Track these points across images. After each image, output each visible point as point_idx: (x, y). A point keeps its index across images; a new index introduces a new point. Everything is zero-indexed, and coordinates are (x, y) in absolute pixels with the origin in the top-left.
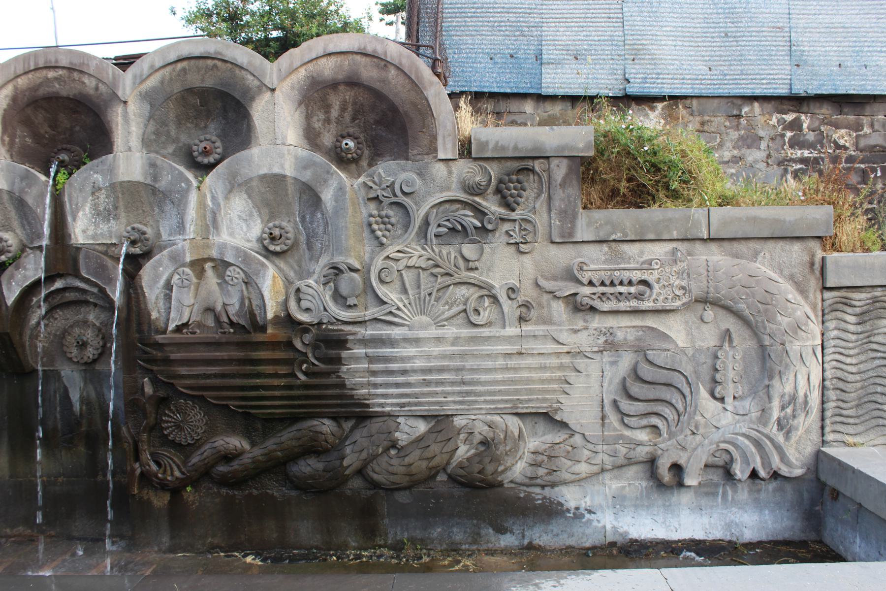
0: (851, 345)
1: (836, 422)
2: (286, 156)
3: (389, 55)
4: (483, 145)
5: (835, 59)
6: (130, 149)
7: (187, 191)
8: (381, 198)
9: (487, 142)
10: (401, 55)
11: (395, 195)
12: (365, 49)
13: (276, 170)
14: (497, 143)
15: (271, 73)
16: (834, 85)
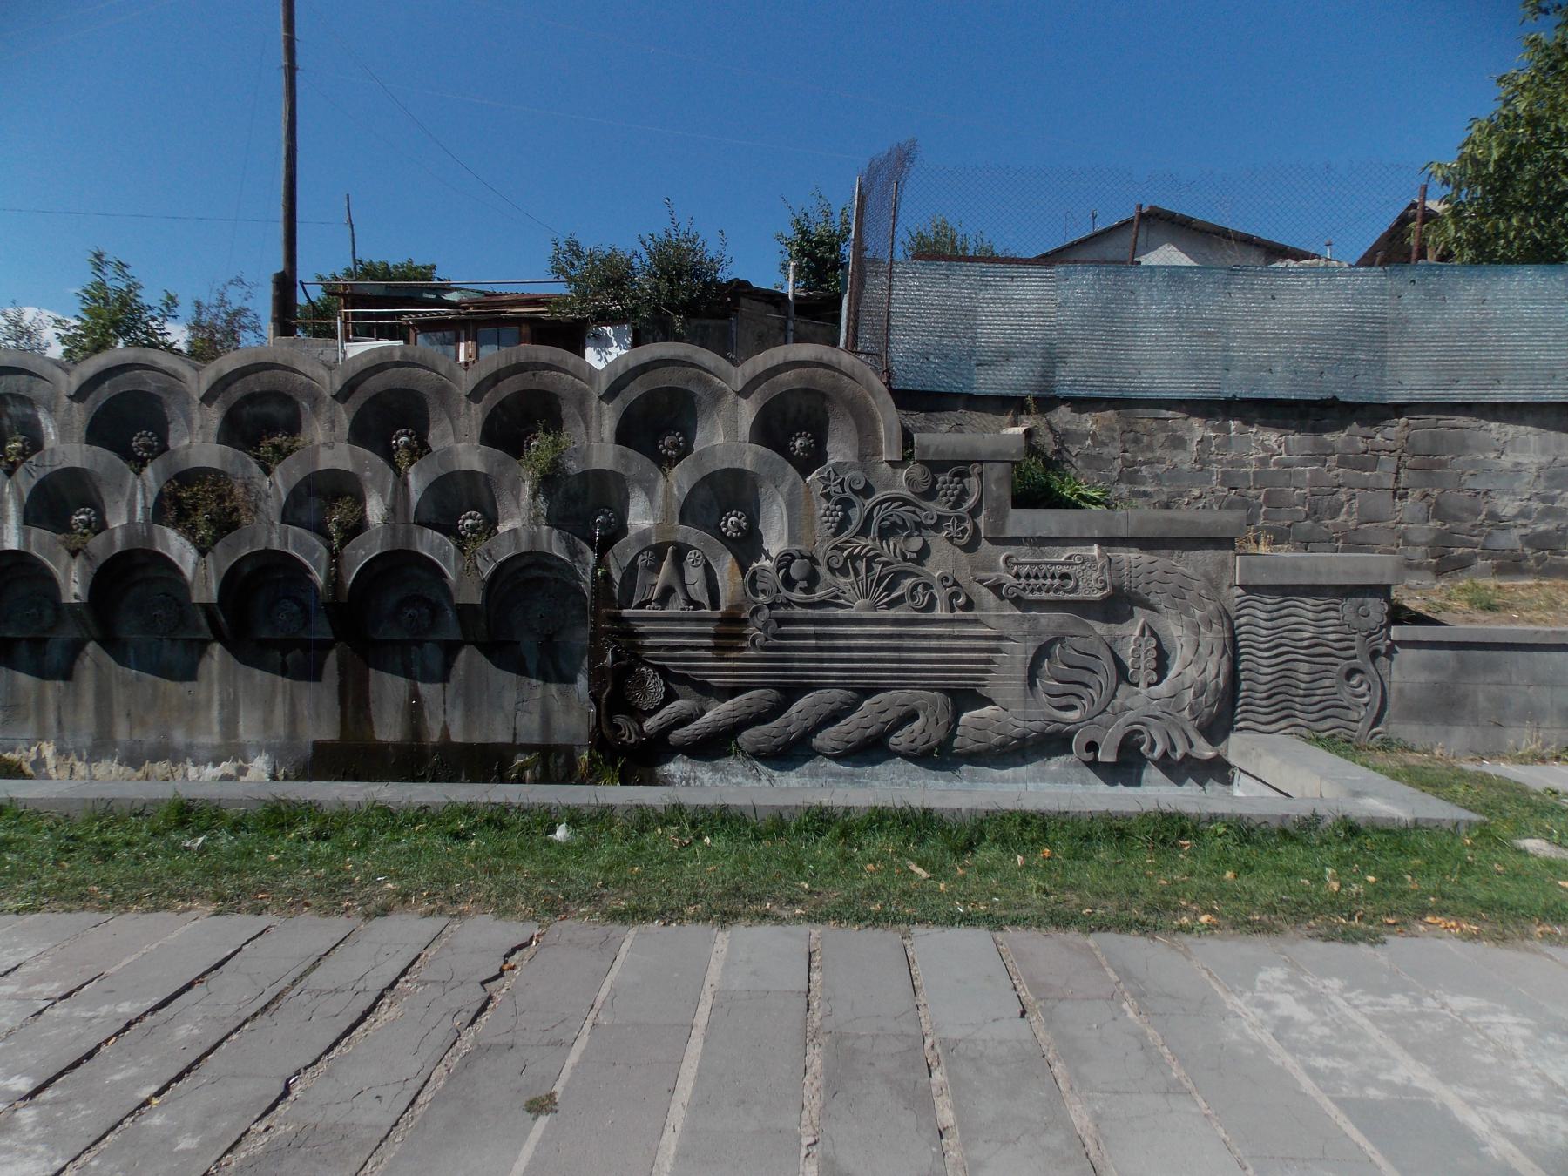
0: (1263, 639)
1: (1246, 711)
2: (747, 453)
3: (843, 364)
4: (925, 449)
5: (1266, 364)
6: (602, 440)
7: (656, 480)
8: (832, 494)
9: (928, 447)
10: (853, 366)
11: (844, 492)
12: (821, 358)
13: (737, 465)
14: (938, 446)
15: (736, 377)
16: (1264, 389)
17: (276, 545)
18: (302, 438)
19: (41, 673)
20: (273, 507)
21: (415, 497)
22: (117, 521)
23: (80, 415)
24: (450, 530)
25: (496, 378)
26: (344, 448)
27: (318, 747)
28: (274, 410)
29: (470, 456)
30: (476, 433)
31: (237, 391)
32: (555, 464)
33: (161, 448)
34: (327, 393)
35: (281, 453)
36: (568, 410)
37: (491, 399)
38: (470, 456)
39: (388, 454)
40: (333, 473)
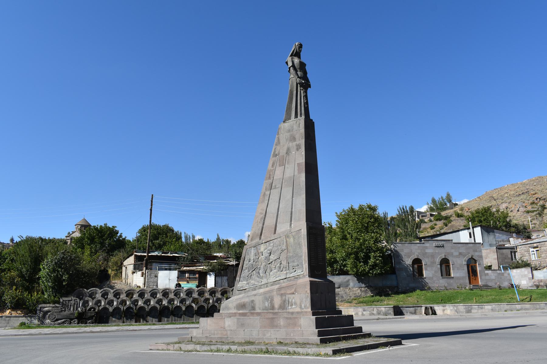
17: (202, 304)
18: (205, 294)
19: (178, 317)
20: (202, 301)
21: (215, 300)
22: (188, 303)
23: (185, 293)
24: (218, 303)
25: (222, 290)
26: (209, 296)
28: (202, 292)
29: (220, 296)
30: (220, 294)
31: (199, 291)
32: (227, 297)
33: (191, 296)
34: (207, 291)
35: (203, 297)
36: (228, 292)
37: (221, 291)
38: (220, 296)
39: (212, 296)
40: (208, 298)
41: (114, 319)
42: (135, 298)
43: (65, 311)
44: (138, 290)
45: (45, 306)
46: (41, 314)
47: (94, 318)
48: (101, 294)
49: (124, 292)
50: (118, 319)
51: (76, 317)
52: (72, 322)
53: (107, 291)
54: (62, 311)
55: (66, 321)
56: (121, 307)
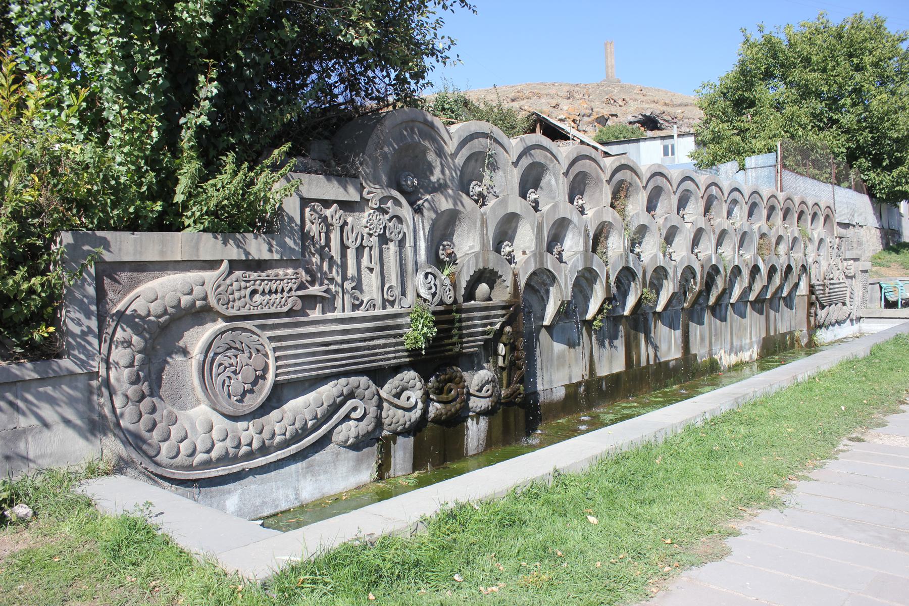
19: (721, 320)
27: (764, 338)
41: (558, 347)
42: (637, 214)
43: (327, 302)
44: (649, 175)
45: (151, 255)
46: (119, 355)
47: (502, 349)
48: (515, 175)
49: (605, 177)
50: (572, 344)
51: (414, 353)
52: (383, 393)
53: (539, 156)
54: (310, 301)
55: (351, 395)
56: (599, 266)
